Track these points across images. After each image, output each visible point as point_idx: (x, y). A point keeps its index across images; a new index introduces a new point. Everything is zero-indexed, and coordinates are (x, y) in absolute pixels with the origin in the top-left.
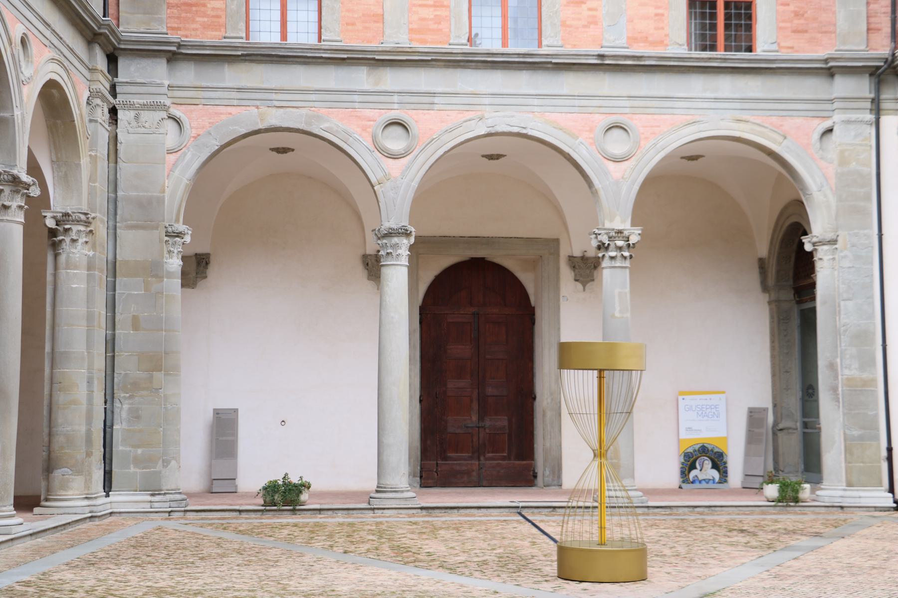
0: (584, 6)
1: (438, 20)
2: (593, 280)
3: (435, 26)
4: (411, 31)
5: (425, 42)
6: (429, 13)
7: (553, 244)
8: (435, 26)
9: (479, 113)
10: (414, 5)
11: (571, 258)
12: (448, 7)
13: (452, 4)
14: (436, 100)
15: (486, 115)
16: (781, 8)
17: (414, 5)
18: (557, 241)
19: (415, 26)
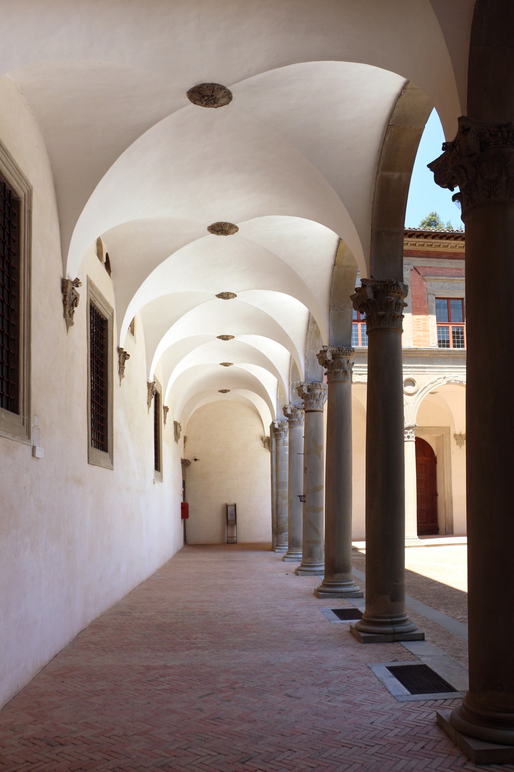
1: (425, 336)
2: (457, 444)
3: (424, 339)
4: (414, 341)
5: (420, 345)
6: (421, 334)
7: (448, 429)
8: (424, 339)
9: (444, 376)
10: (415, 330)
11: (455, 435)
12: (429, 331)
13: (430, 330)
14: (426, 370)
15: (447, 376)
17: (415, 330)
18: (449, 428)
19: (415, 339)
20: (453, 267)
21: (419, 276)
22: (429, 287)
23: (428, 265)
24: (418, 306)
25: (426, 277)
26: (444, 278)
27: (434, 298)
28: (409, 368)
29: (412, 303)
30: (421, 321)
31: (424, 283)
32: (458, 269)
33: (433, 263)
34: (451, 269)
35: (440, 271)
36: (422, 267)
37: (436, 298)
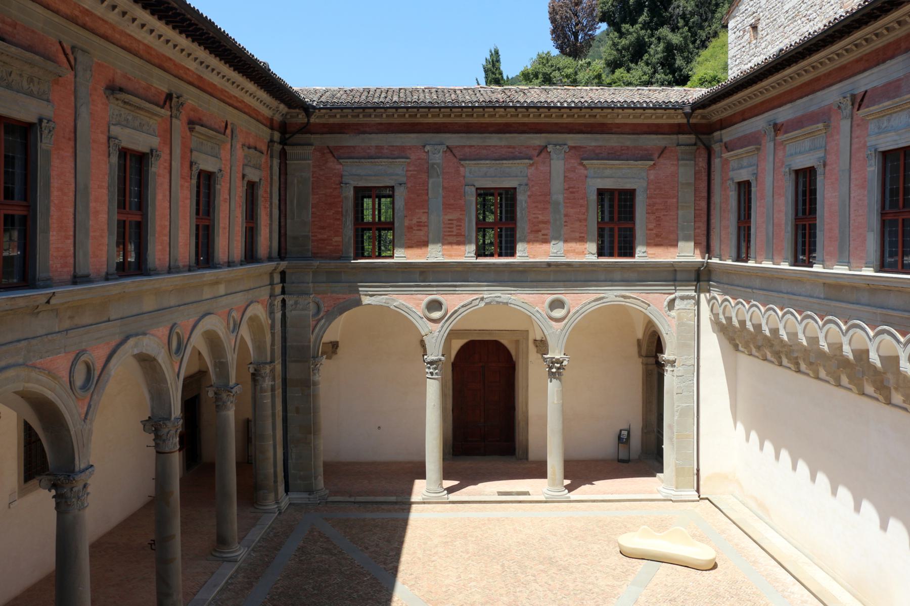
0: (540, 233)
16: (649, 232)
20: (503, 143)
21: (455, 160)
22: (467, 174)
23: (468, 143)
24: (452, 202)
25: (462, 162)
26: (488, 162)
27: (474, 189)
28: (437, 286)
29: (444, 197)
30: (455, 222)
31: (462, 169)
32: (509, 147)
33: (475, 140)
34: (501, 147)
35: (484, 152)
36: (457, 147)
37: (477, 189)
